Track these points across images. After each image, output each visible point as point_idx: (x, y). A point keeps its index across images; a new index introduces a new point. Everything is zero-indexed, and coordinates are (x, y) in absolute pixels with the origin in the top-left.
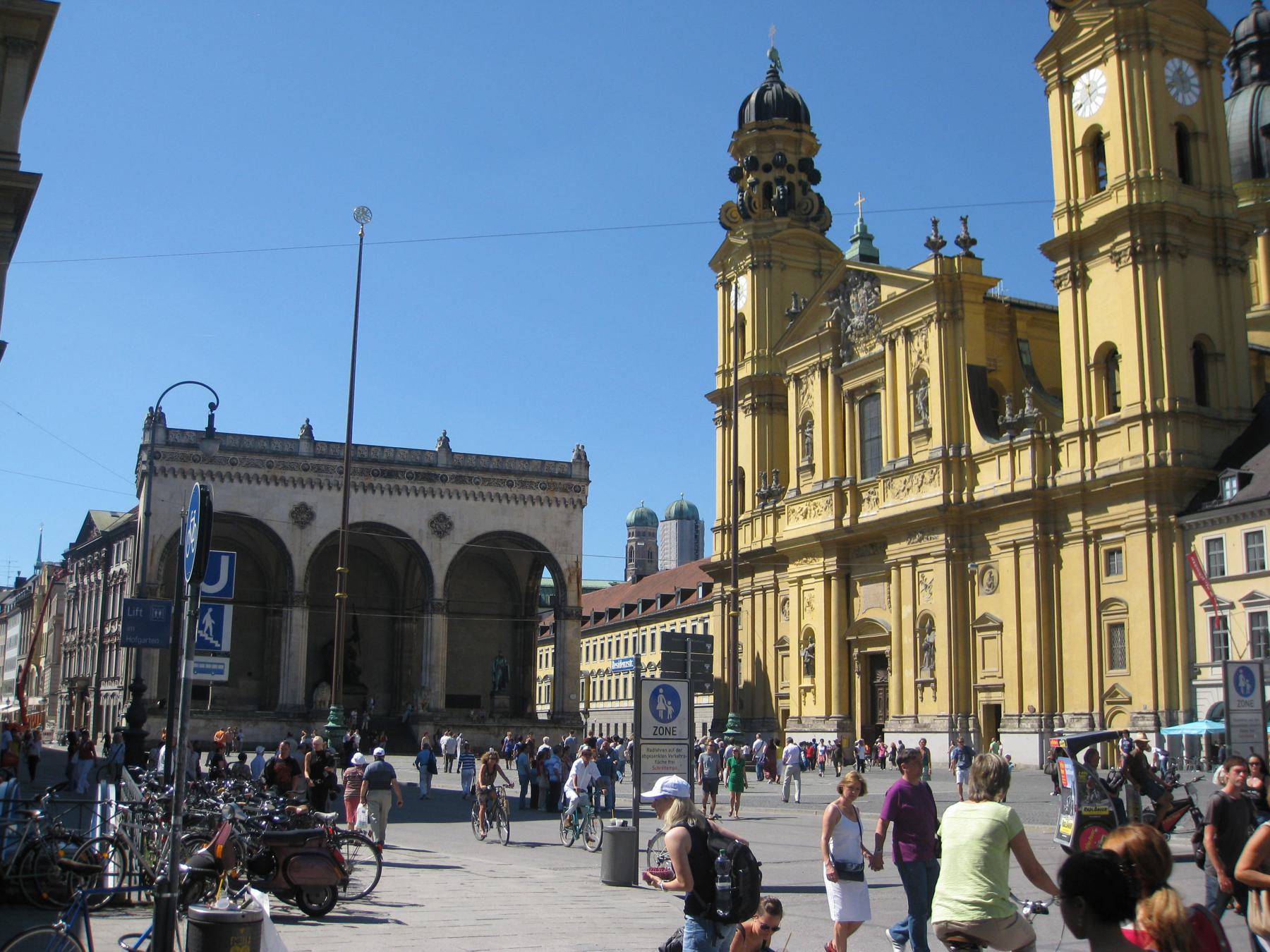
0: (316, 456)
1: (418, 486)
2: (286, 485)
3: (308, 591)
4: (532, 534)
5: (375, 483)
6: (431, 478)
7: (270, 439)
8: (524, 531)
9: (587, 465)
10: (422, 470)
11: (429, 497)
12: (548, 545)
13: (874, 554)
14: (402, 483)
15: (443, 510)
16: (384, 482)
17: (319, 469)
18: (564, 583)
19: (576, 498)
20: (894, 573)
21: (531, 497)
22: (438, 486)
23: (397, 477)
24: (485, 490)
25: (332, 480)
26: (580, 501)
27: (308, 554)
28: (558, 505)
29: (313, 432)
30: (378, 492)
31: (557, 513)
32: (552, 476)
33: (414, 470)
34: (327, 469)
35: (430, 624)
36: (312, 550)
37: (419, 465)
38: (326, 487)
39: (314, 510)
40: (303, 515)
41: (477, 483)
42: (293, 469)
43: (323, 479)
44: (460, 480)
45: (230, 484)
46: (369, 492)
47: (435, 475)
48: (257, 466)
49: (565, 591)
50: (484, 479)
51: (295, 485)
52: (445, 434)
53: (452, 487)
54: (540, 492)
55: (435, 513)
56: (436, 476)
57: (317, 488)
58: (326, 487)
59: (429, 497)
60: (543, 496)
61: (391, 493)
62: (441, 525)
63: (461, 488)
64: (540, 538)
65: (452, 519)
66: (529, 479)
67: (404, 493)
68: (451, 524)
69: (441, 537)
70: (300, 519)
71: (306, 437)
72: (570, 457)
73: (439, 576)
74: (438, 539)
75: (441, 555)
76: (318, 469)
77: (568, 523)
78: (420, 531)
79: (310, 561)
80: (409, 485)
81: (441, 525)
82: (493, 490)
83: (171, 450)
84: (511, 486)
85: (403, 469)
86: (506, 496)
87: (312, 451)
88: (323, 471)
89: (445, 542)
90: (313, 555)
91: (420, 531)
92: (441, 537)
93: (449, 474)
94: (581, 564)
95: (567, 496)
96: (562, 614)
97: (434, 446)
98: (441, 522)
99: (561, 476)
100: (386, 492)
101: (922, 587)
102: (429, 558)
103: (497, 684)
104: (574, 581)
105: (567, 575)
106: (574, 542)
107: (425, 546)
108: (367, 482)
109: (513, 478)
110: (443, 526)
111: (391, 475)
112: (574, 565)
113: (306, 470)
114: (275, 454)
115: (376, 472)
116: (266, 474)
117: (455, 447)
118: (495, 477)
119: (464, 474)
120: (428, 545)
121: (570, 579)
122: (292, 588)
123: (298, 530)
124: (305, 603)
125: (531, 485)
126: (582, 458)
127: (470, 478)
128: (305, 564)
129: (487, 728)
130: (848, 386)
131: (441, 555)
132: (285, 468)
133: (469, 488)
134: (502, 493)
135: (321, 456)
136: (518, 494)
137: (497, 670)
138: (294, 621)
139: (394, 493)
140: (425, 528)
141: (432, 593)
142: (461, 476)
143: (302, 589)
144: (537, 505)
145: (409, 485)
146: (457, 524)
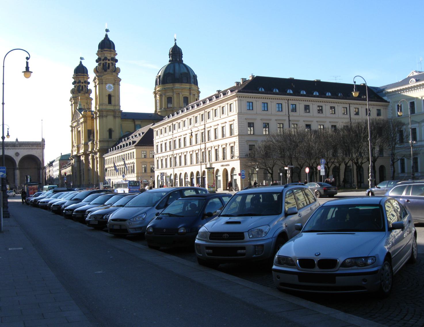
6: (15, 146)
8: (33, 154)
9: (44, 141)
12: (38, 157)
14: (9, 148)
21: (34, 148)
22: (16, 147)
23: (8, 147)
24: (25, 148)
31: (39, 151)
32: (38, 144)
37: (12, 144)
44: (20, 146)
53: (19, 147)
54: (35, 147)
55: (16, 152)
59: (15, 149)
61: (7, 149)
62: (17, 154)
63: (20, 148)
68: (19, 154)
72: (40, 140)
73: (17, 163)
75: (17, 160)
78: (13, 156)
80: (11, 148)
81: (17, 154)
82: (26, 148)
84: (30, 146)
89: (18, 157)
91: (13, 156)
93: (18, 145)
97: (15, 141)
100: (7, 150)
117: (19, 141)
125: (34, 146)
126: (43, 140)
131: (17, 160)
133: (22, 147)
140: (14, 155)
144: (35, 149)
145: (11, 148)
146: (20, 154)
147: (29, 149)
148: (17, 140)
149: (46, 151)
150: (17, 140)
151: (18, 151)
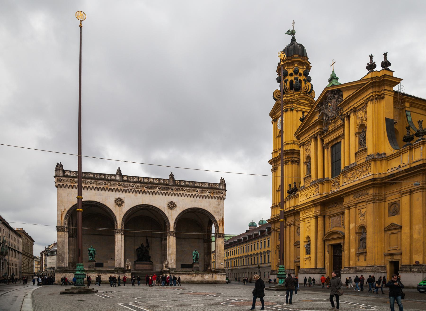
0: (123, 181)
1: (162, 192)
2: (112, 191)
3: (123, 229)
4: (206, 209)
5: (146, 191)
6: (167, 189)
7: (105, 175)
8: (203, 208)
10: (164, 186)
11: (167, 196)
12: (212, 213)
13: (337, 206)
15: (172, 200)
16: (149, 191)
17: (124, 185)
18: (218, 225)
19: (221, 196)
20: (347, 211)
25: (129, 189)
26: (223, 197)
27: (122, 216)
28: (215, 199)
29: (122, 172)
30: (148, 194)
33: (160, 186)
34: (128, 186)
35: (169, 240)
36: (124, 214)
38: (128, 192)
39: (124, 200)
40: (119, 202)
41: (185, 191)
42: (114, 185)
43: (126, 189)
44: (178, 190)
45: (90, 191)
46: (144, 194)
47: (169, 188)
48: (100, 184)
49: (218, 228)
50: (187, 189)
51: (116, 191)
52: (172, 173)
55: (169, 201)
56: (169, 188)
57: (124, 192)
58: (128, 192)
59: (167, 196)
60: (209, 195)
61: (153, 194)
62: (172, 205)
63: (178, 193)
64: (209, 210)
65: (176, 204)
66: (204, 189)
67: (157, 194)
68: (175, 205)
69: (172, 210)
70: (118, 203)
71: (119, 174)
74: (171, 210)
76: (124, 186)
77: (219, 205)
79: (123, 218)
81: (172, 205)
83: (66, 178)
85: (156, 185)
86: (195, 195)
87: (121, 179)
88: (126, 186)
89: (174, 211)
90: (124, 216)
92: (172, 210)
94: (224, 219)
95: (218, 196)
96: (217, 236)
98: (172, 204)
99: (216, 189)
101: (360, 216)
102: (168, 217)
103: (194, 260)
104: (221, 225)
105: (219, 223)
106: (221, 211)
107: (166, 213)
108: (143, 190)
109: (198, 189)
110: (173, 206)
111: (152, 188)
112: (221, 219)
113: (119, 186)
114: (108, 180)
115: (146, 186)
116: (104, 187)
118: (191, 189)
119: (179, 188)
120: (167, 212)
121: (220, 224)
122: (117, 227)
123: (118, 207)
124: (122, 233)
127: (182, 189)
128: (122, 219)
129: (191, 274)
130: (326, 141)
132: (111, 185)
134: (194, 194)
135: (125, 181)
136: (200, 195)
137: (194, 255)
138: (118, 239)
139: (153, 194)
140: (166, 206)
141: (169, 229)
142: (178, 188)
143: (121, 228)
144: (207, 198)
145: (159, 191)
146: (178, 205)
147: (195, 197)
148: (172, 176)
149: (228, 204)
150: (172, 176)
151: (174, 199)
